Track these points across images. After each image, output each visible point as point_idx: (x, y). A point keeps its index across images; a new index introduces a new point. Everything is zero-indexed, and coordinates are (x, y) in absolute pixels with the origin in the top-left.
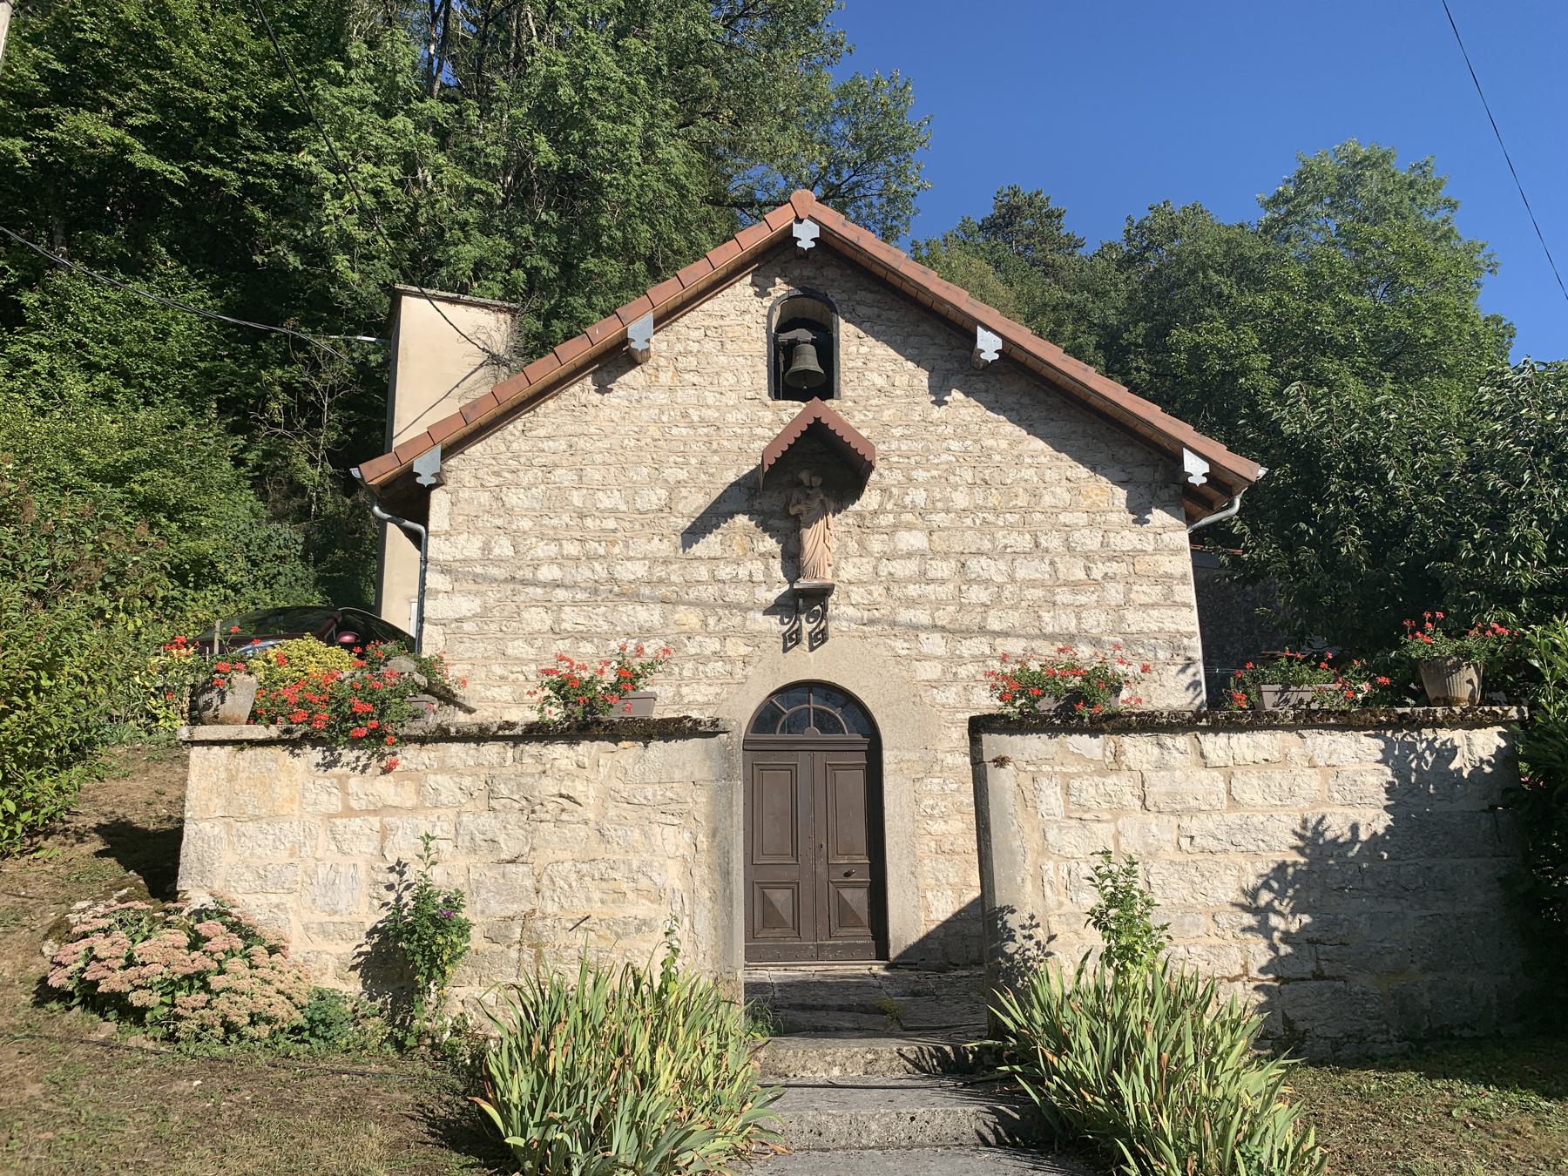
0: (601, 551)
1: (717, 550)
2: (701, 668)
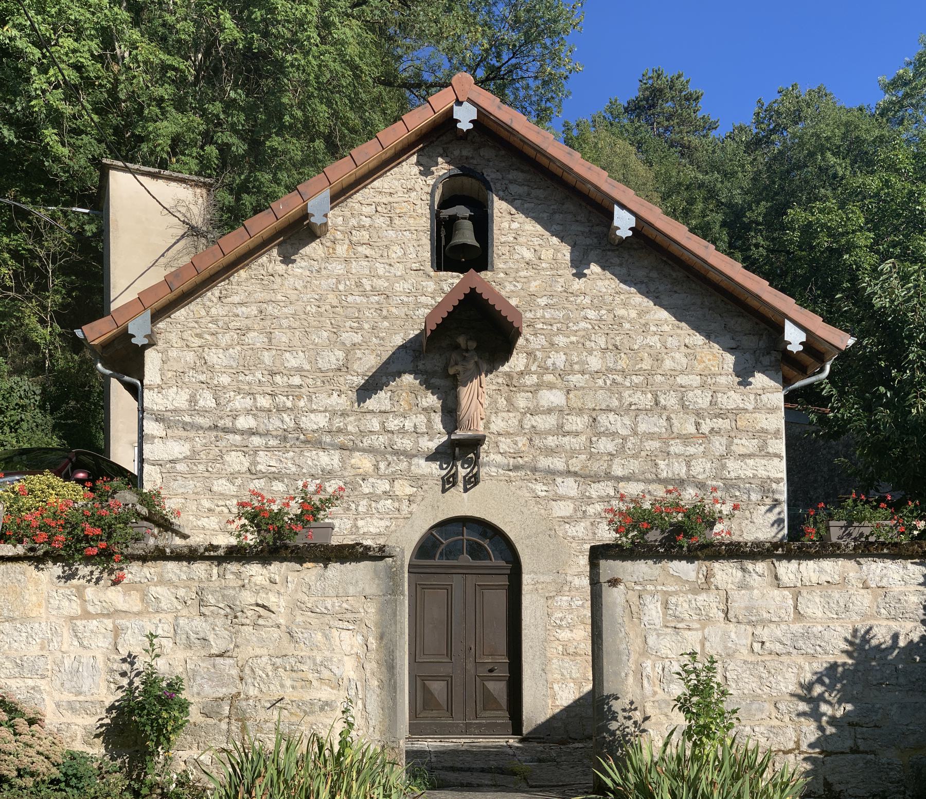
0: (289, 404)
2: (374, 505)
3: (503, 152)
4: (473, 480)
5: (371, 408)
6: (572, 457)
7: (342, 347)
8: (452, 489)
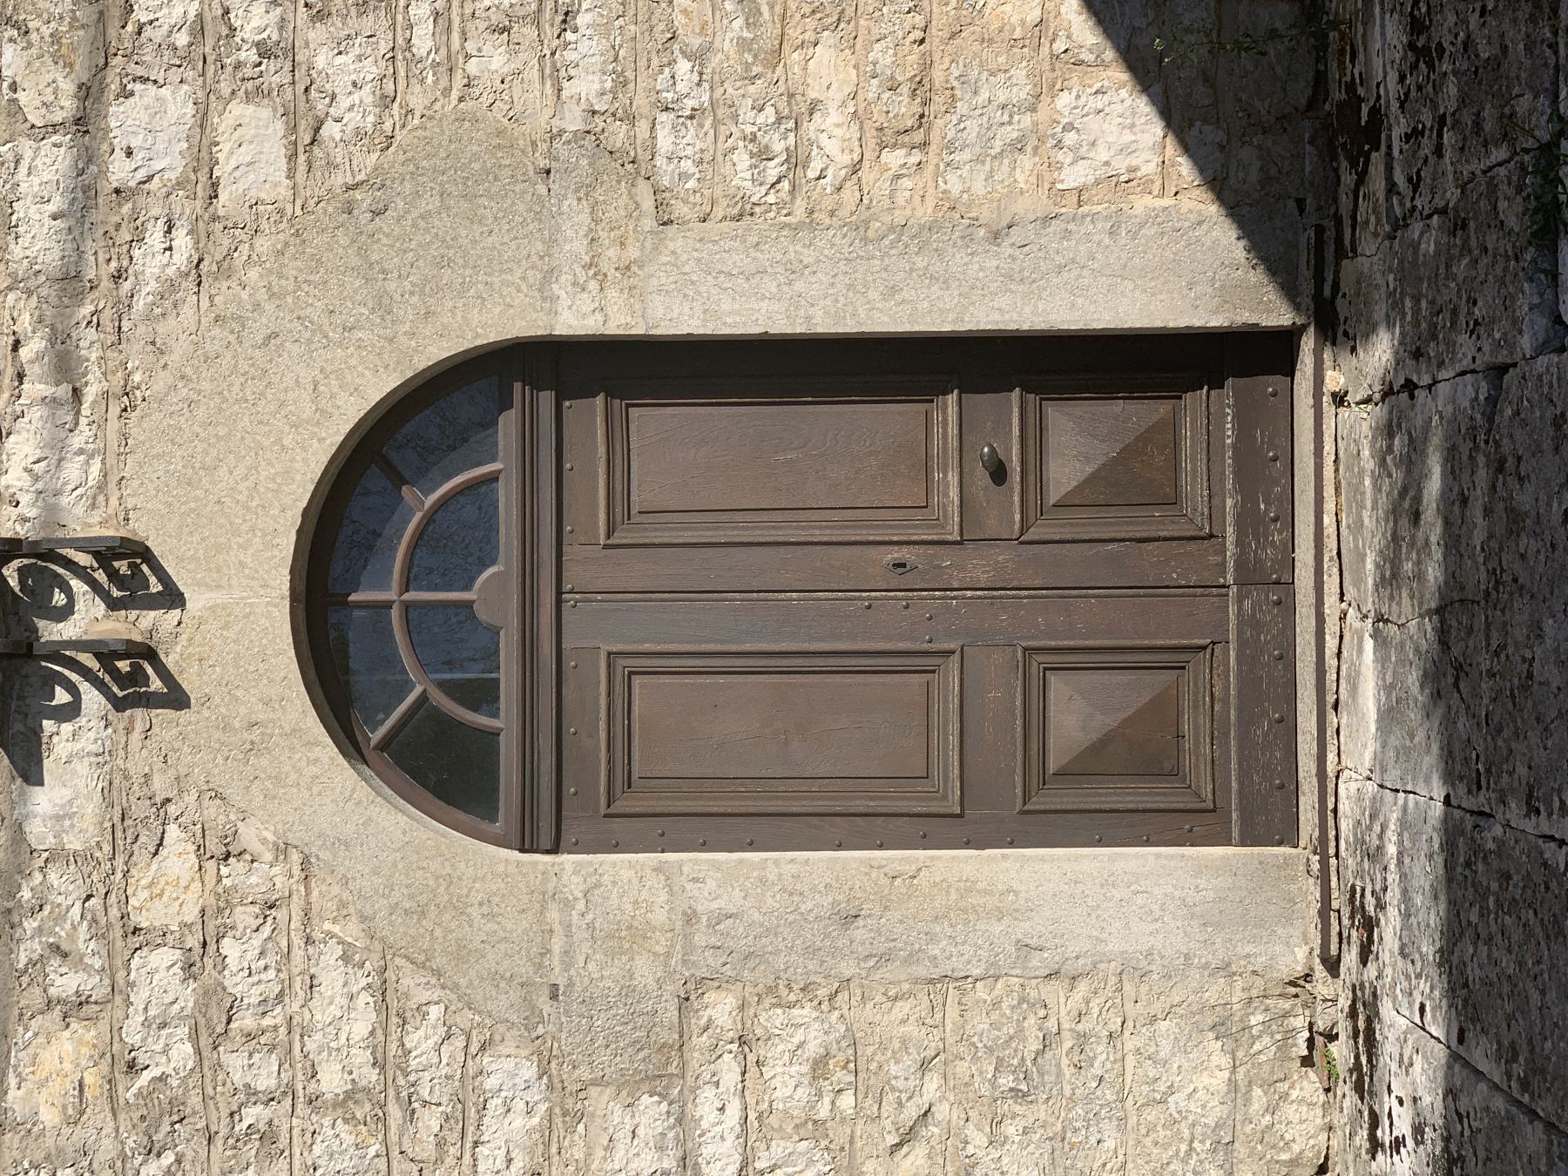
2: (245, 1021)
4: (122, 566)
8: (170, 661)
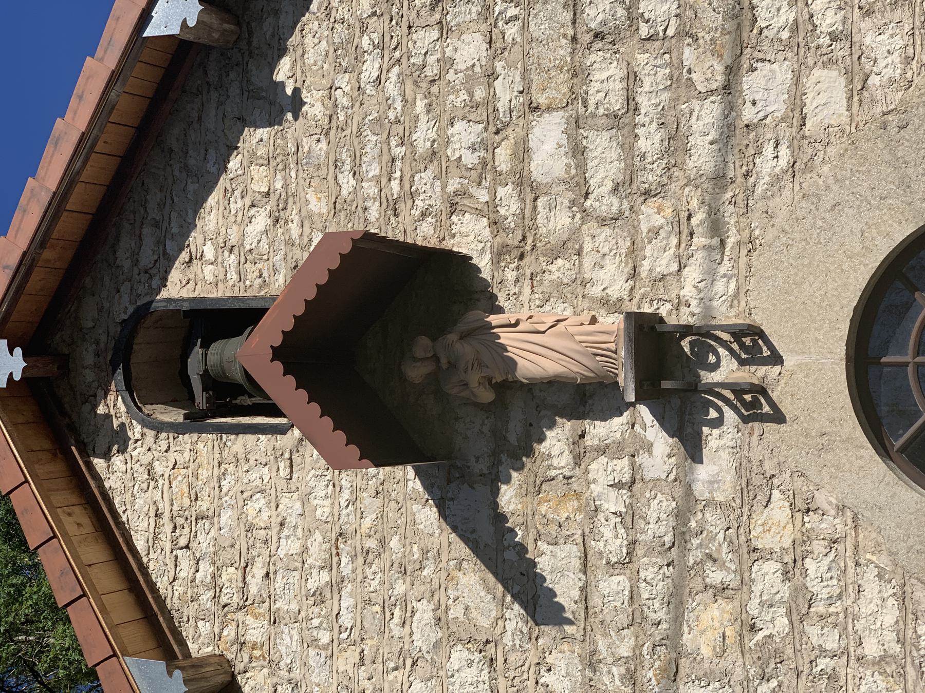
1: (569, 554)
2: (819, 608)
3: (88, 281)
4: (747, 341)
5: (576, 594)
6: (690, 83)
7: (445, 650)
8: (774, 396)
